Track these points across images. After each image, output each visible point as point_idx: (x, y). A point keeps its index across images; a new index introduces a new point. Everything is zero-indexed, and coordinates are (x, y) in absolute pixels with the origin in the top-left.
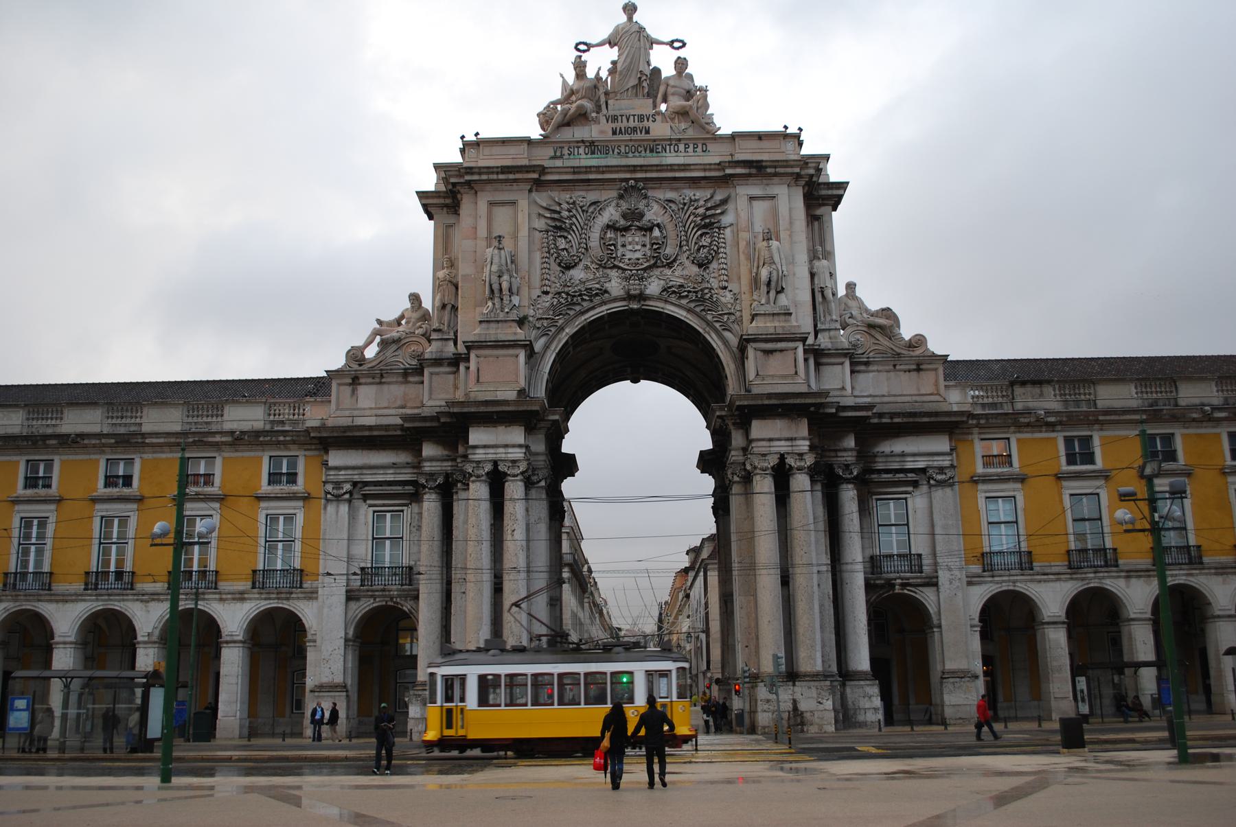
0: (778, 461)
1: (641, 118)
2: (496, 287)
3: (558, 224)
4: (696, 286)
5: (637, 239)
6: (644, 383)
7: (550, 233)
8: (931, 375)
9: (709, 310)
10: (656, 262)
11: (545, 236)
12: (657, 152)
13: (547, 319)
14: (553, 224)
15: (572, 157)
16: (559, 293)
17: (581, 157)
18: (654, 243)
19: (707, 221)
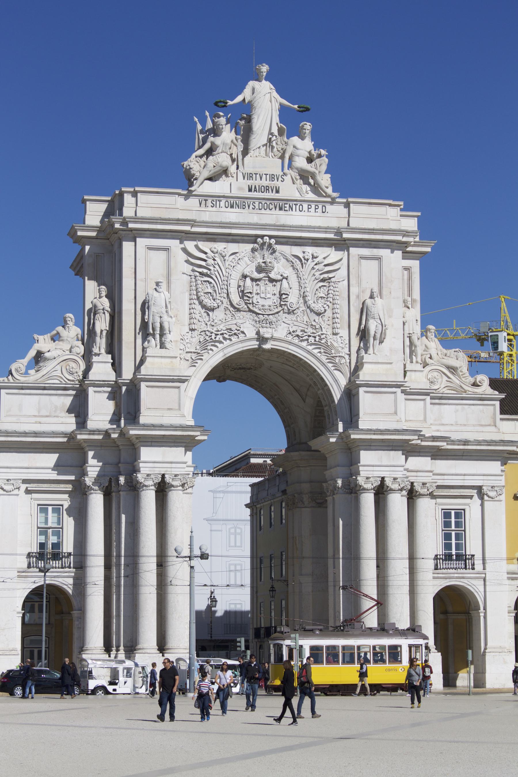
0: (379, 482)
1: (272, 177)
2: (158, 325)
3: (205, 271)
4: (314, 331)
5: (269, 289)
6: (228, 381)
7: (197, 278)
8: (492, 407)
9: (325, 352)
10: (283, 309)
11: (193, 280)
12: (285, 210)
13: (194, 353)
14: (200, 270)
15: (214, 208)
16: (205, 331)
17: (221, 210)
18: (282, 294)
19: (326, 276)
